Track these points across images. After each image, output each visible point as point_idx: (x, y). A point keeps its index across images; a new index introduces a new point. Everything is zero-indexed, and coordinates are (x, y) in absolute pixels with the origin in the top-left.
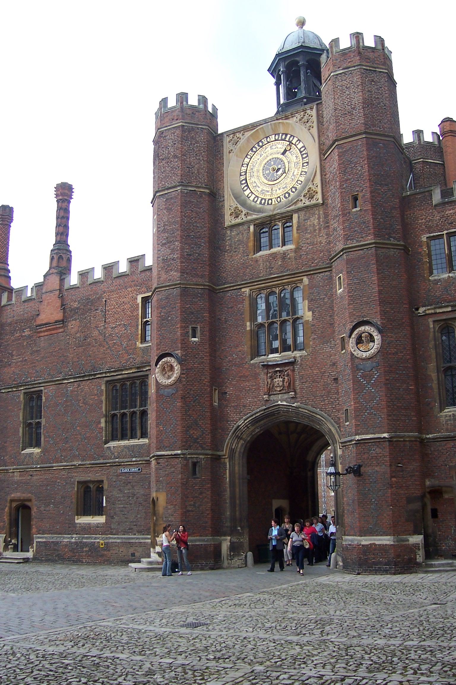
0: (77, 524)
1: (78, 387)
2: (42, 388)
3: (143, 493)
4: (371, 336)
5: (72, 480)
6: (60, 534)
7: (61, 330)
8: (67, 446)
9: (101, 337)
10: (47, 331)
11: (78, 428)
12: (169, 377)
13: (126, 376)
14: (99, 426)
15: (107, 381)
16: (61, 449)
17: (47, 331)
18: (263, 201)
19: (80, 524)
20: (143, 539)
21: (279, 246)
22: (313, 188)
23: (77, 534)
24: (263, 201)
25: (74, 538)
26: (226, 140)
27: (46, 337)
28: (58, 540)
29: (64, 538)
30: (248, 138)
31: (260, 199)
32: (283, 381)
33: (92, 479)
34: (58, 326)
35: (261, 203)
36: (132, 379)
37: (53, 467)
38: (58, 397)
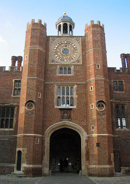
3: (10, 148)
4: (102, 105)
12: (30, 109)
13: (6, 106)
18: (61, 60)
20: (9, 165)
21: (66, 74)
22: (79, 60)
24: (61, 60)
26: (50, 38)
30: (58, 40)
31: (60, 59)
32: (67, 115)
35: (61, 60)
36: (8, 107)
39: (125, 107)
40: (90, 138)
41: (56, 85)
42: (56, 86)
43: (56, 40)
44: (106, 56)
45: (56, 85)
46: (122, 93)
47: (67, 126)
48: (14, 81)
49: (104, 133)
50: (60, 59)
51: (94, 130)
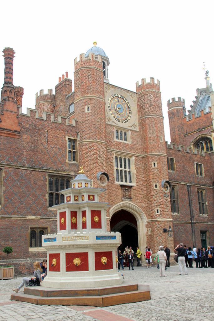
0: (30, 252)
1: (30, 174)
2: (3, 168)
4: (167, 186)
5: (26, 226)
6: (17, 259)
7: (17, 137)
8: (22, 206)
9: (45, 150)
10: (7, 134)
11: (30, 197)
13: (60, 175)
14: (44, 198)
15: (49, 175)
16: (17, 207)
17: (7, 134)
19: (32, 252)
23: (30, 258)
25: (29, 261)
27: (6, 137)
28: (18, 262)
29: (23, 261)
31: (115, 118)
33: (40, 227)
34: (16, 134)
36: (63, 177)
37: (12, 217)
38: (15, 176)
39: (175, 189)
40: (154, 223)
41: (114, 153)
42: (114, 154)
43: (110, 90)
44: (170, 131)
45: (114, 153)
46: (174, 173)
47: (129, 208)
48: (67, 138)
49: (169, 218)
50: (115, 118)
51: (159, 214)
